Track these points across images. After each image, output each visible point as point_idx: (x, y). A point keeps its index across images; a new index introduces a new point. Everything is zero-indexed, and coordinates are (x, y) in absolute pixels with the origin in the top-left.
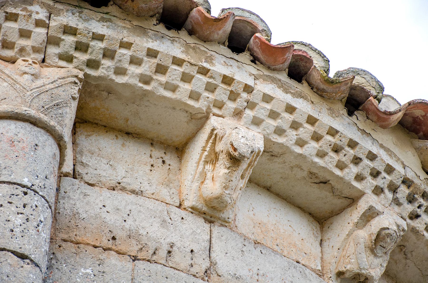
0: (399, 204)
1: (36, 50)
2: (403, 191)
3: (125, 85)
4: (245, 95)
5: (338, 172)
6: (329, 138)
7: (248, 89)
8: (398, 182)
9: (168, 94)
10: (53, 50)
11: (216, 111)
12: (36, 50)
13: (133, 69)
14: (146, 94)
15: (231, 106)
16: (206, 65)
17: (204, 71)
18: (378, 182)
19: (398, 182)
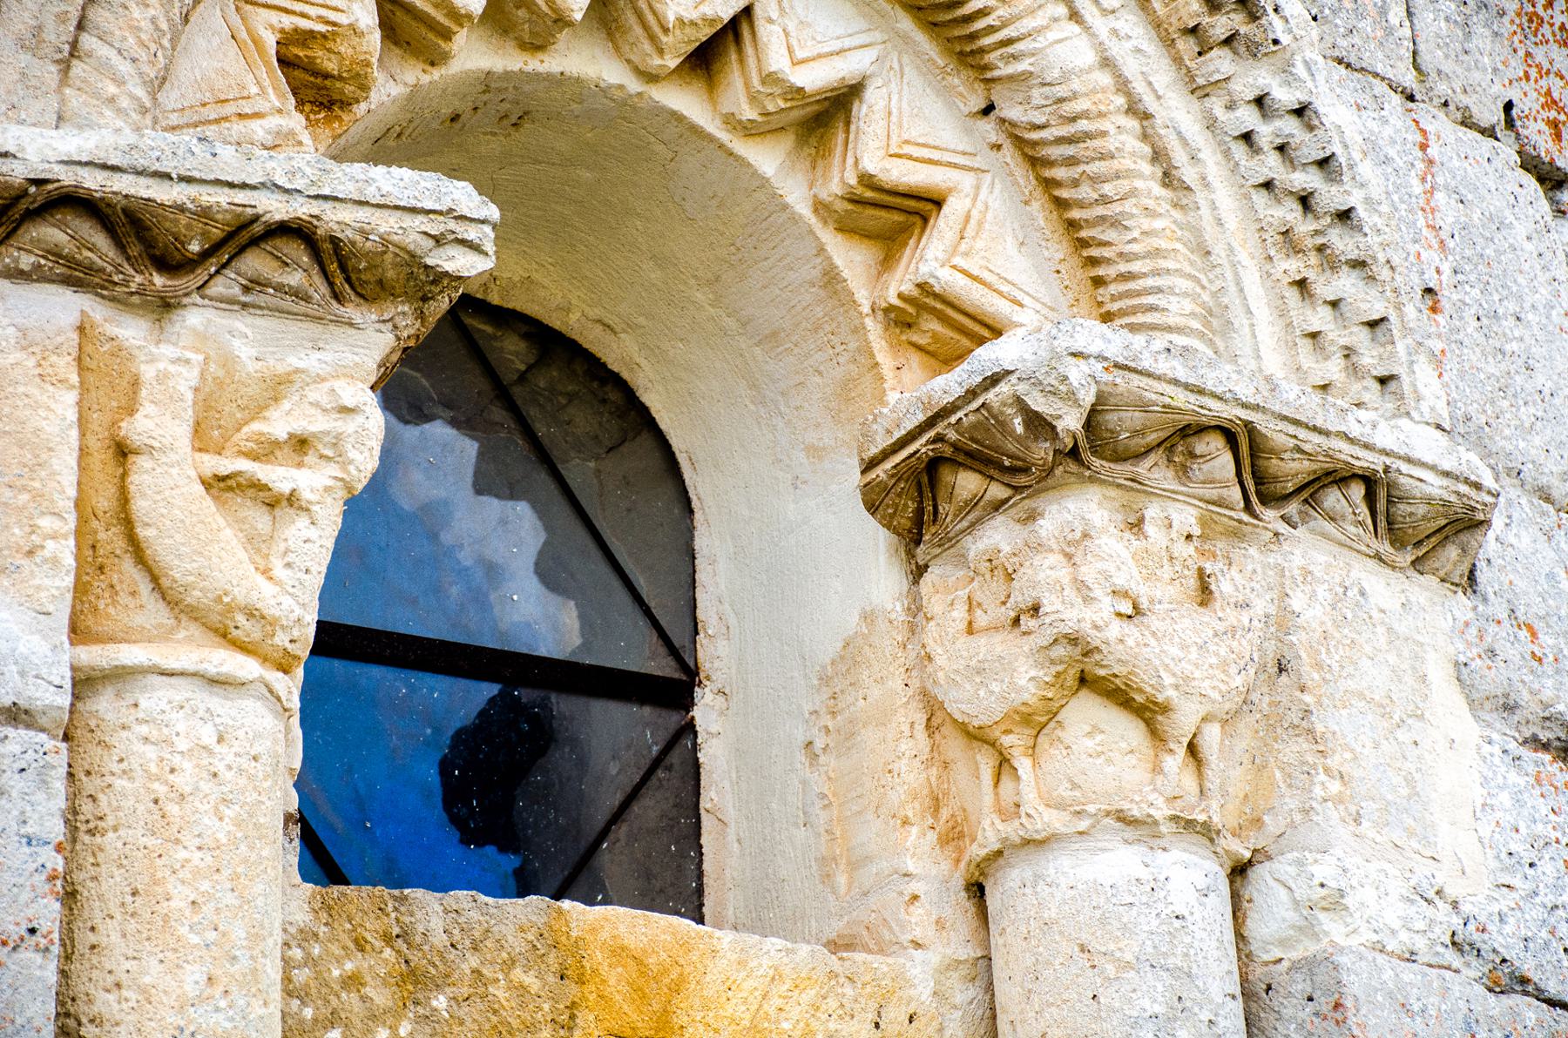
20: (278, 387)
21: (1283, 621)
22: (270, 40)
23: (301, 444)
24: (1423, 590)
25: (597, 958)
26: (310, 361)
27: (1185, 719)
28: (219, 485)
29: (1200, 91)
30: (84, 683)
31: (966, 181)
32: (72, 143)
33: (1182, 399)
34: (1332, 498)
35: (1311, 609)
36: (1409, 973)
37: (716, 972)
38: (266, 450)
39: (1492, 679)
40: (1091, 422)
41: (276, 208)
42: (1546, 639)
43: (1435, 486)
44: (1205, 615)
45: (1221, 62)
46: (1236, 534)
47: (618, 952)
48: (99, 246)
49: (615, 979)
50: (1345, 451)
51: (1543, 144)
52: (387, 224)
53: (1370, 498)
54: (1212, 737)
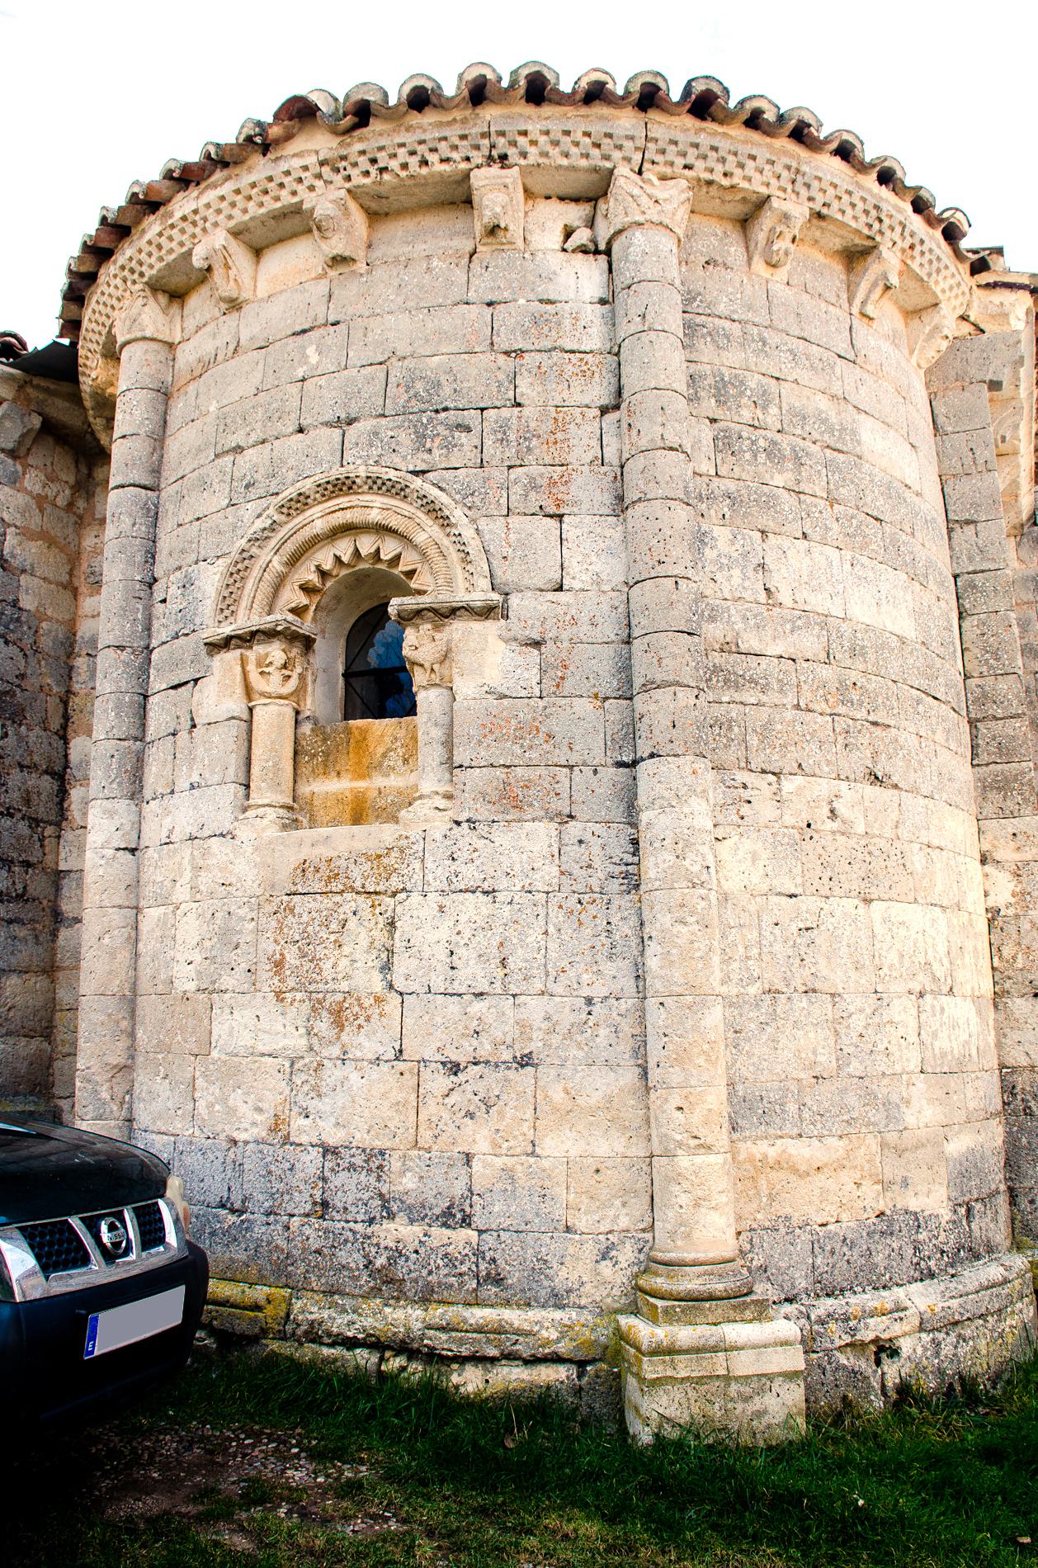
0: (331, 182)
1: (125, 291)
2: (326, 170)
3: (160, 271)
4: (197, 218)
5: (278, 205)
6: (255, 190)
7: (196, 212)
8: (317, 169)
9: (173, 256)
10: (129, 283)
11: (196, 241)
12: (125, 291)
13: (153, 260)
14: (168, 265)
15: (198, 231)
16: (170, 222)
17: (172, 226)
18: (306, 183)
19: (317, 169)
20: (267, 655)
21: (449, 642)
22: (297, 588)
23: (271, 663)
24: (489, 623)
25: (354, 730)
26: (270, 649)
27: (427, 665)
28: (262, 673)
29: (448, 535)
30: (251, 710)
31: (419, 565)
32: (233, 627)
33: (415, 607)
34: (458, 613)
35: (456, 636)
36: (473, 702)
37: (375, 728)
38: (267, 666)
39: (511, 634)
40: (399, 615)
41: (254, 629)
42: (530, 622)
43: (479, 604)
44: (433, 644)
45: (448, 530)
46: (443, 625)
47: (357, 728)
48: (239, 642)
49: (356, 733)
50: (454, 604)
51: (552, 510)
52: (268, 626)
53: (466, 609)
54: (436, 667)
